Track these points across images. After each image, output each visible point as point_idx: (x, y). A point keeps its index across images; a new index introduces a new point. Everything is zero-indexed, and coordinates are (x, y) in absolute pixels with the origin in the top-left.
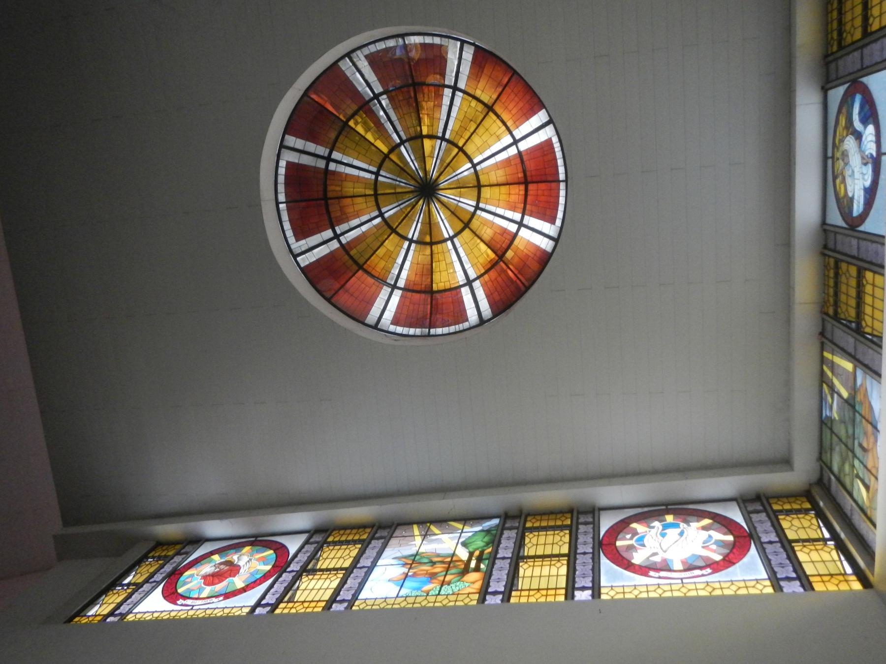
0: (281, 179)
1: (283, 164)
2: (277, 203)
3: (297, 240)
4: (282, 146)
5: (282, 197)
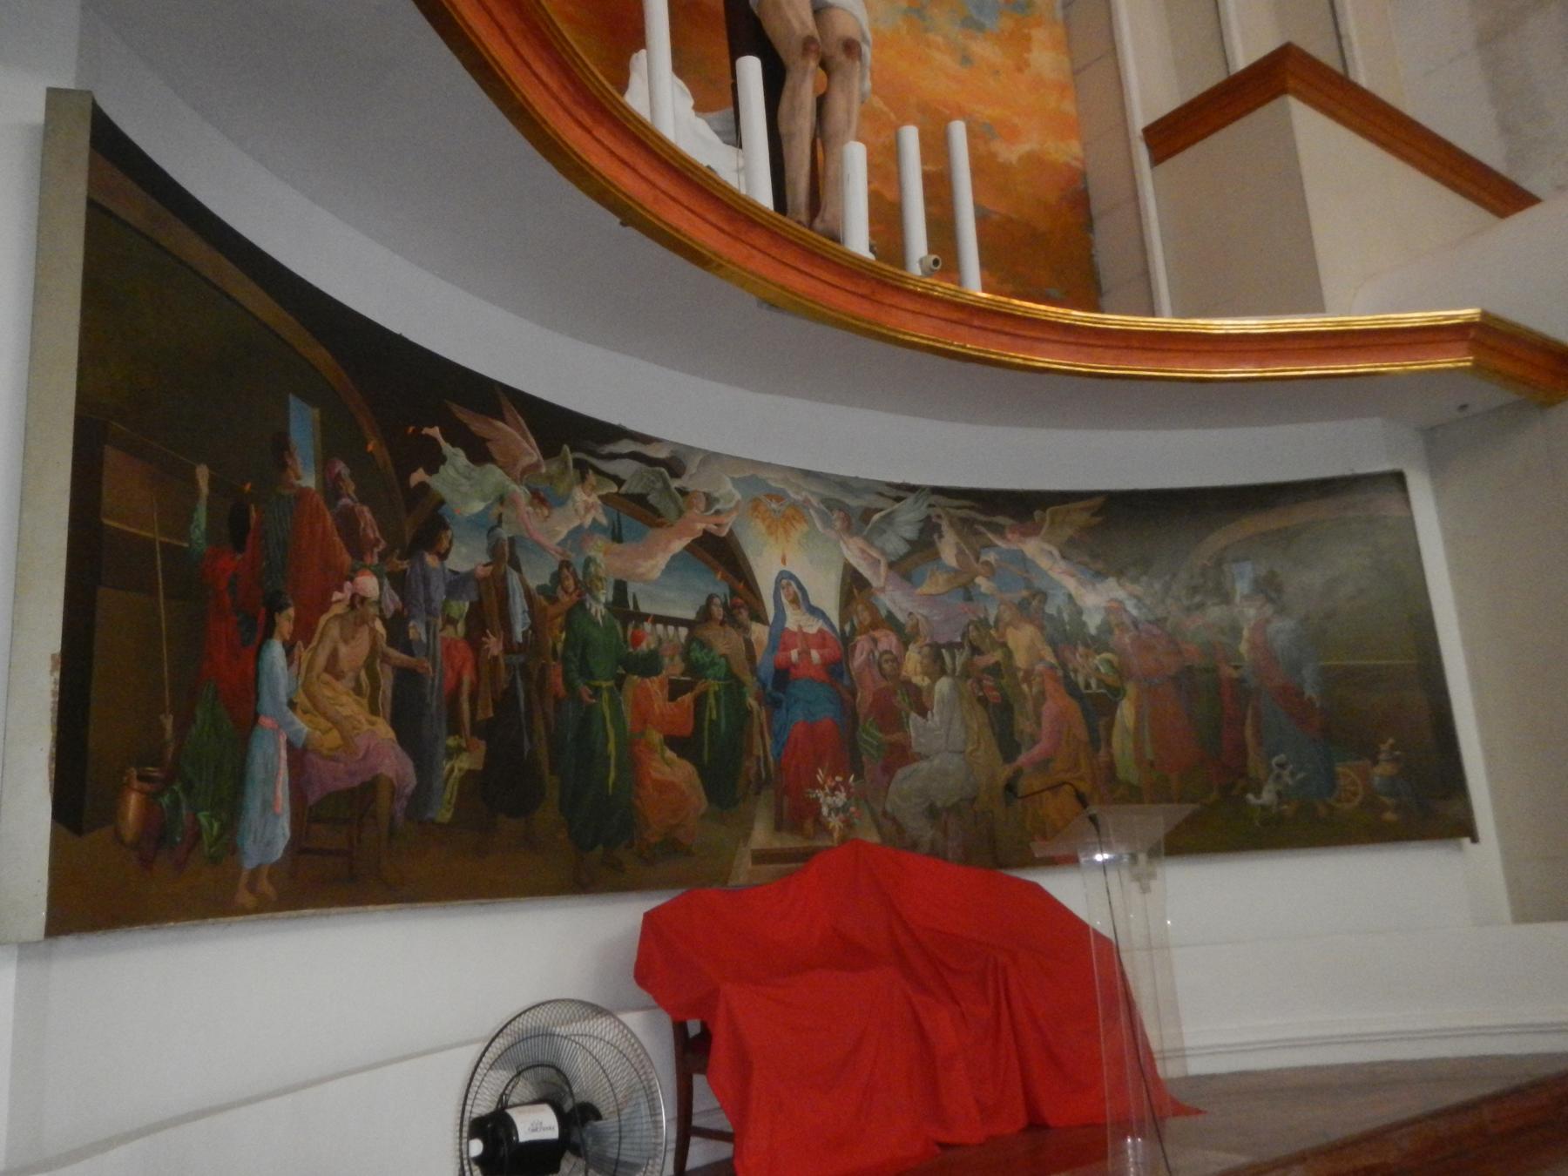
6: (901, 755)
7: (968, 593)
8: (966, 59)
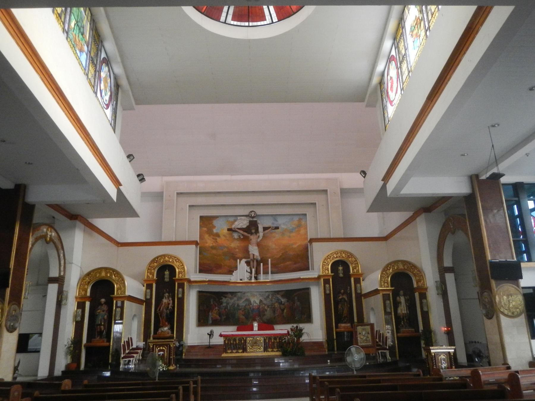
0: (239, 23)
1: (232, 22)
2: (249, 26)
3: (266, 20)
4: (225, 23)
5: (247, 24)
6: (265, 315)
7: (272, 301)
8: (290, 237)
